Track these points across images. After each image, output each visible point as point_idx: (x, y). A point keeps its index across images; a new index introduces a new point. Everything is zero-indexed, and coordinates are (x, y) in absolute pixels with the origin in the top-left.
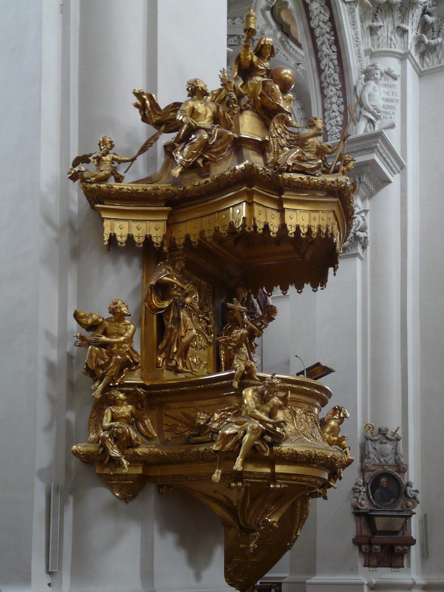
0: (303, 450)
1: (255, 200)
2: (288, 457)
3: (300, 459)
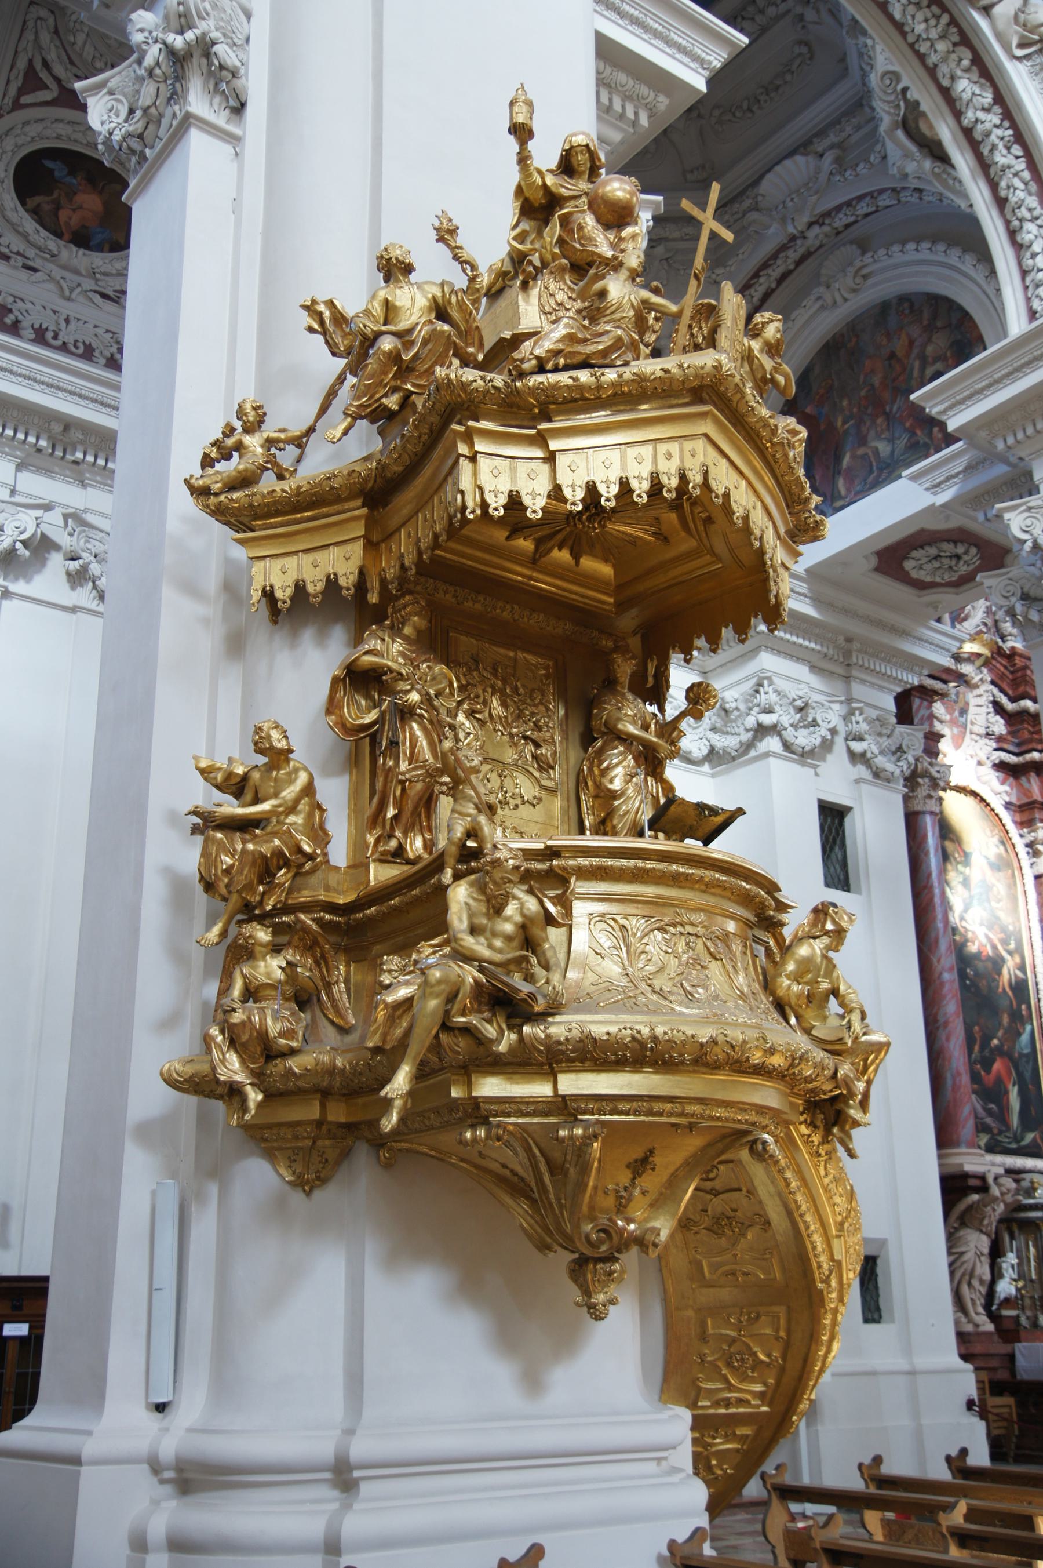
0: (613, 1029)
1: (478, 447)
2: (572, 1051)
3: (615, 1054)
